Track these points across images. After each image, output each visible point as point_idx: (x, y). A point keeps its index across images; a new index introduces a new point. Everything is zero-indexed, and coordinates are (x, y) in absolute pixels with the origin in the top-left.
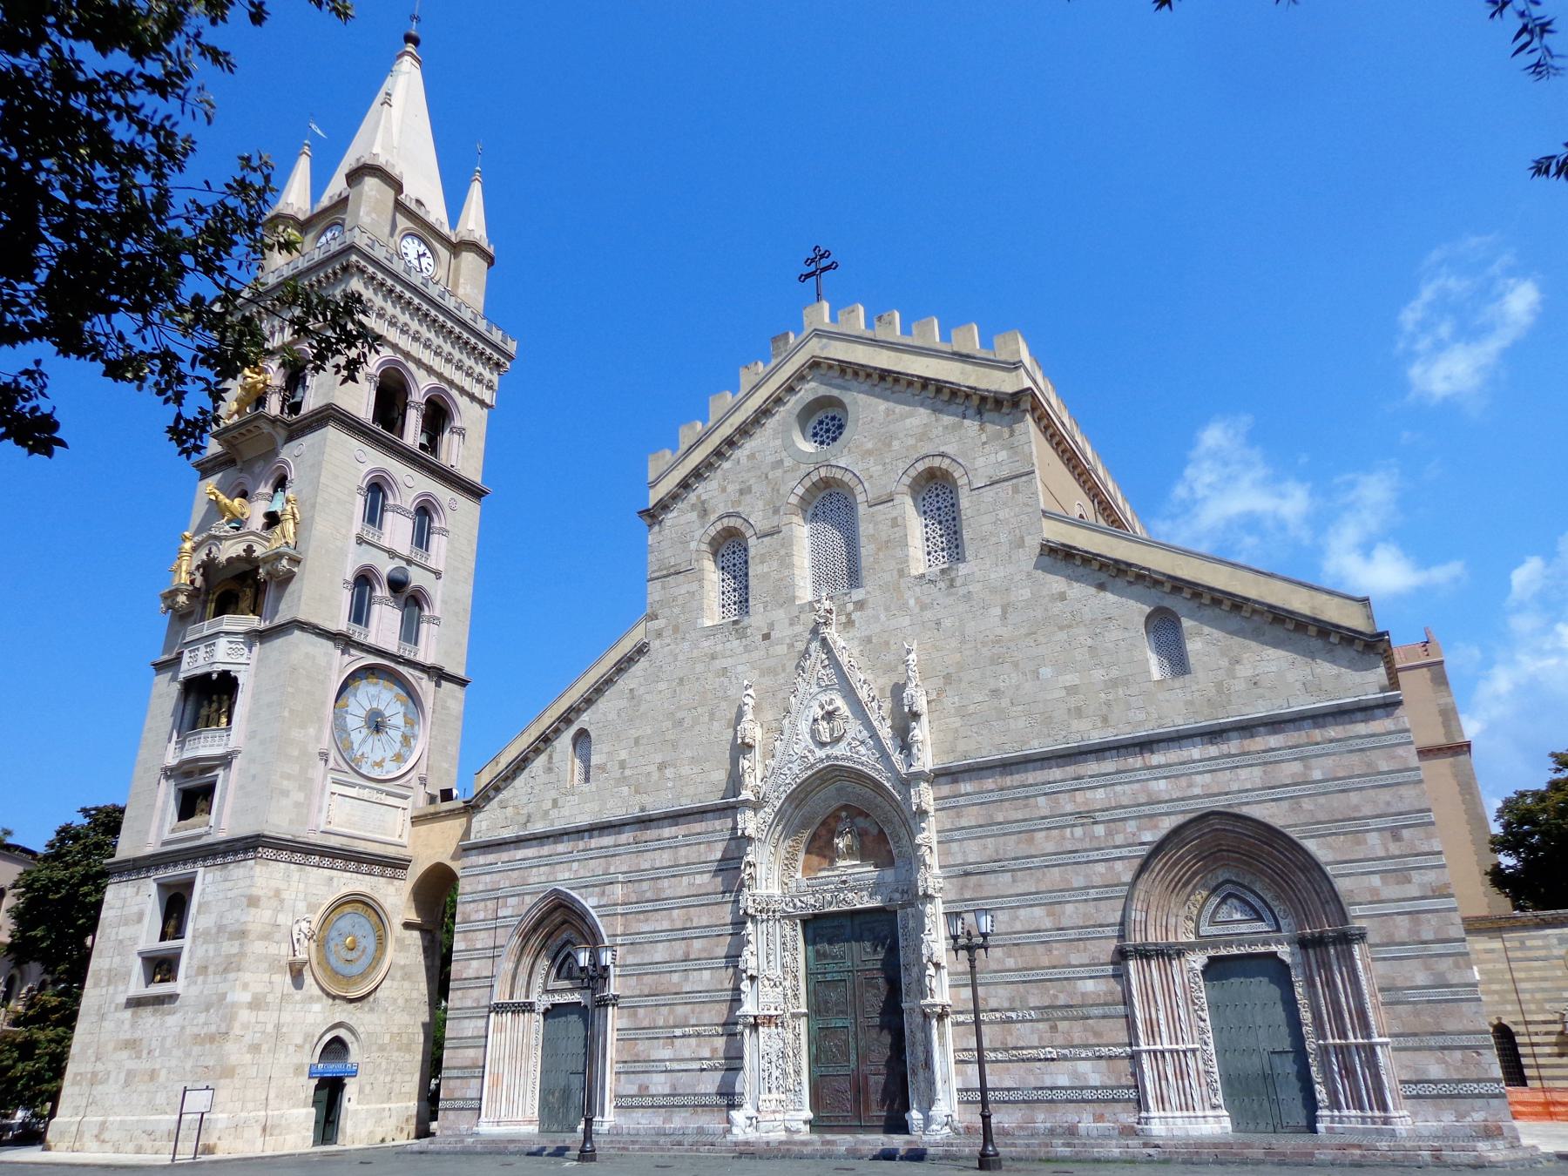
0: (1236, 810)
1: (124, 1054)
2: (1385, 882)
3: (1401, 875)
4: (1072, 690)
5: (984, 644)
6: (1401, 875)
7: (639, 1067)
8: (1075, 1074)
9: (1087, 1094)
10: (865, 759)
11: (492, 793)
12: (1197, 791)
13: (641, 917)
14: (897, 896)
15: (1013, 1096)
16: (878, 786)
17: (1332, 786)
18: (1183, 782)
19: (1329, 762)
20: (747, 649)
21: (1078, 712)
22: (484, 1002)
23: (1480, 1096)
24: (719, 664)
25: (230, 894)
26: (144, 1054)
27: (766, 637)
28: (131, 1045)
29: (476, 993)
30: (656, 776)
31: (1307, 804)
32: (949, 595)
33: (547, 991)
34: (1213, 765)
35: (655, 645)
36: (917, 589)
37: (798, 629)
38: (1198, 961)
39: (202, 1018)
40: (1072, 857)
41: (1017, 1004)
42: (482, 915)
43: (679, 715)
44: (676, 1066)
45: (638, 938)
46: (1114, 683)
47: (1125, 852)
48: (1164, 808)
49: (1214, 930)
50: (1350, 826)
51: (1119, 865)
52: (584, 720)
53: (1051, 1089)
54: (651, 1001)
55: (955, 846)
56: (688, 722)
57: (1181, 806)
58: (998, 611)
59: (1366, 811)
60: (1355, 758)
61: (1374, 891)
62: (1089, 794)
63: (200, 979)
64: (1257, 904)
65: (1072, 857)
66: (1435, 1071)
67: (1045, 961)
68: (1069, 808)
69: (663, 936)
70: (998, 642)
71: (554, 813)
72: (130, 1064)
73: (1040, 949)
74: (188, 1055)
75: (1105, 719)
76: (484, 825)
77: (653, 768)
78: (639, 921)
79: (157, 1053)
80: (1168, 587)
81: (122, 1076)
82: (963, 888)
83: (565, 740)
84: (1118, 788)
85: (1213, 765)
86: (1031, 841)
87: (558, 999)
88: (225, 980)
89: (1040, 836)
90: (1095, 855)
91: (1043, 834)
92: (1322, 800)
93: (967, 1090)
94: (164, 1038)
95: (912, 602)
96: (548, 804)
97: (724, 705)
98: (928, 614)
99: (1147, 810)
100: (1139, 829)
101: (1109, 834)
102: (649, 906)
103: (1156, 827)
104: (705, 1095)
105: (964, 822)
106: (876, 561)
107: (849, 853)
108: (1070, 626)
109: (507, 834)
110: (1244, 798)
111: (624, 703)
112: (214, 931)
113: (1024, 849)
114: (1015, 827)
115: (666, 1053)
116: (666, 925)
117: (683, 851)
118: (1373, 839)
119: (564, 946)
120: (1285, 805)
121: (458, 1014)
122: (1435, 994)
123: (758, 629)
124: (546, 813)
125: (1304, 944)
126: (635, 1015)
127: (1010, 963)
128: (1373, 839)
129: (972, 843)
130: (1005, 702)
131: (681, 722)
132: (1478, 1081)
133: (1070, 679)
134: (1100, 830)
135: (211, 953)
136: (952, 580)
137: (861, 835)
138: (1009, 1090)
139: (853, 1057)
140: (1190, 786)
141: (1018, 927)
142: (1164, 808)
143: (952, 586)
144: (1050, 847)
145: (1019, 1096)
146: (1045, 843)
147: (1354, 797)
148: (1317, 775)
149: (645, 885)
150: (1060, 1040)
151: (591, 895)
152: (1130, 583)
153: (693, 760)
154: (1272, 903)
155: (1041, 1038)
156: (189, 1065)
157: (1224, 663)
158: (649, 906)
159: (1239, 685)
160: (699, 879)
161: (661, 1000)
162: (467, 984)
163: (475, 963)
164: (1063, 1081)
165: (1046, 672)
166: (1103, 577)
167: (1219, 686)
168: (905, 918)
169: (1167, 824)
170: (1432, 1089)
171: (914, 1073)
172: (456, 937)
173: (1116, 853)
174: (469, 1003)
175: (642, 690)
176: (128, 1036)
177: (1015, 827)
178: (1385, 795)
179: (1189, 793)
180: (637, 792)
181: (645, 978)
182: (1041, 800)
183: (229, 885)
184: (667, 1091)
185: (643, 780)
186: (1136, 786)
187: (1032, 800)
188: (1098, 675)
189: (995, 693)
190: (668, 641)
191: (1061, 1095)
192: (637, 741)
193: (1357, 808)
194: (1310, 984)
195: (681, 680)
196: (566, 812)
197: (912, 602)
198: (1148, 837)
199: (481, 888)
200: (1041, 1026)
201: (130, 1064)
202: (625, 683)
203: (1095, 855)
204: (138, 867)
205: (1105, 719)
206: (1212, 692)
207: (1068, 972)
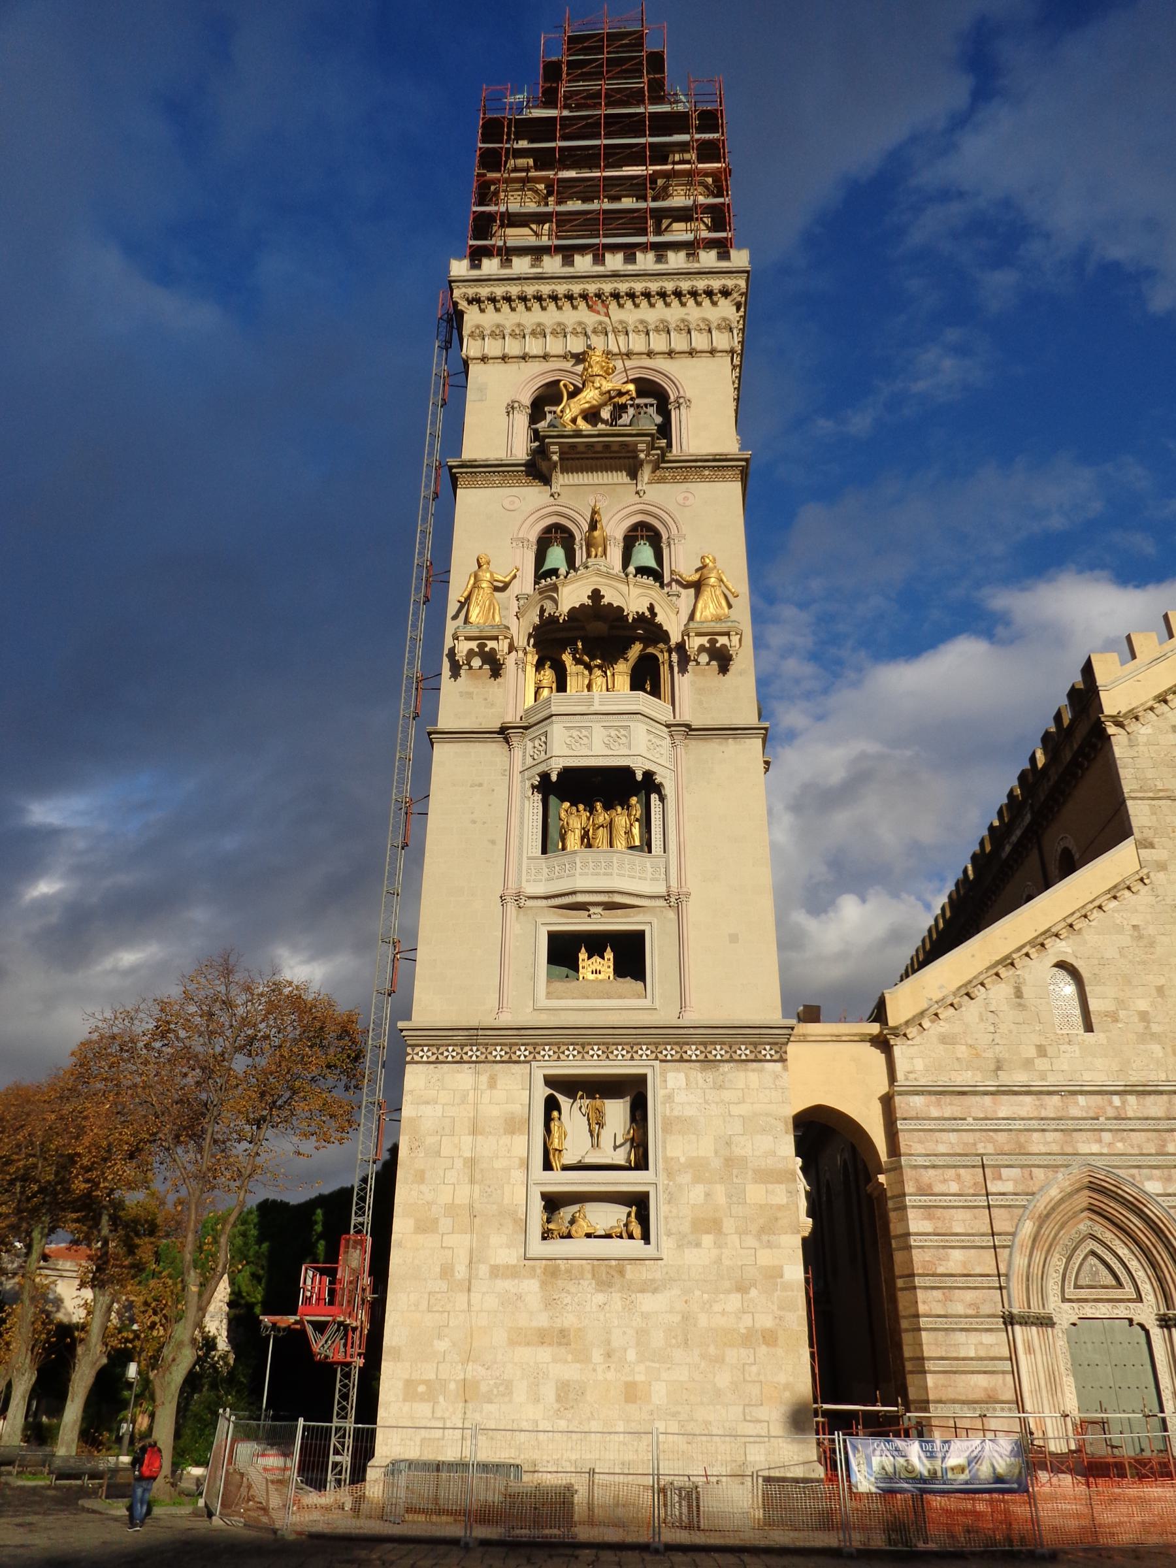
1: (544, 1354)
11: (926, 1023)
22: (986, 1309)
25: (735, 1110)
26: (597, 1356)
28: (562, 1337)
29: (969, 1296)
33: (1065, 1300)
35: (1158, 877)
39: (734, 1301)
42: (954, 1188)
63: (707, 1240)
71: (1041, 1064)
72: (571, 1372)
74: (720, 1360)
76: (919, 1065)
79: (631, 1355)
81: (549, 1393)
87: (1089, 1310)
88: (769, 1245)
96: (1032, 1052)
109: (965, 1078)
111: (1125, 940)
112: (716, 1163)
119: (1082, 1240)
121: (941, 1323)
124: (1028, 1064)
135: (721, 1199)
151: (1149, 1178)
156: (723, 1379)
162: (949, 1282)
163: (957, 1254)
172: (911, 1214)
174: (960, 1309)
175: (1151, 930)
176: (543, 1320)
183: (727, 1095)
192: (1160, 990)
196: (1063, 1064)
199: (942, 1149)
201: (571, 1372)
204: (474, 1043)
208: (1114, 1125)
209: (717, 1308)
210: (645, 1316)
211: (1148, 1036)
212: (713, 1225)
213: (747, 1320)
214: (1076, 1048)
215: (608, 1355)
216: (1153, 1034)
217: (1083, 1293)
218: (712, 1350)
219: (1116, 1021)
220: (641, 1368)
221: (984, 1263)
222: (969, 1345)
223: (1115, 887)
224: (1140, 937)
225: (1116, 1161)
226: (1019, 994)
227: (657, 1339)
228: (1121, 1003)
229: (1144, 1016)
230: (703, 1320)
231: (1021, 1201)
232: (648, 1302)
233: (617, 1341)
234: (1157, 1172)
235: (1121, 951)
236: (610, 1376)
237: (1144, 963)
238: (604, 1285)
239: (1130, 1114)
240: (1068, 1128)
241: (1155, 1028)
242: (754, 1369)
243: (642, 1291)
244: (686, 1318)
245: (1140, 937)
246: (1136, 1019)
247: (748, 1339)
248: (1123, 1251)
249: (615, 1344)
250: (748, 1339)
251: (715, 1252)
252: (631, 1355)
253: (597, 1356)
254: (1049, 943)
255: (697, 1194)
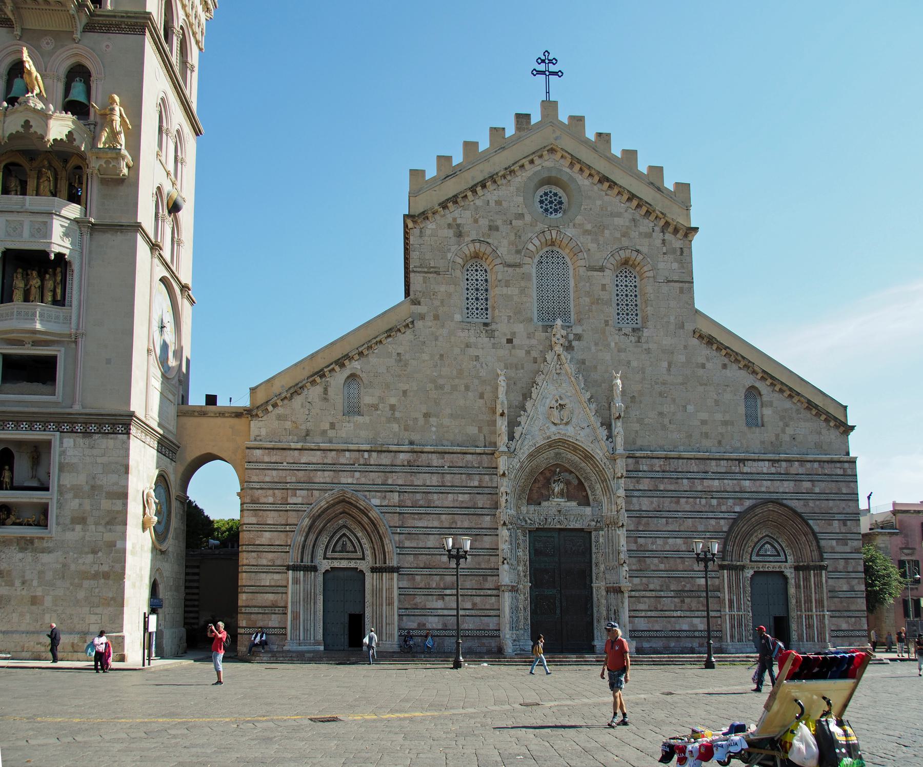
0: (785, 502)
2: (837, 544)
3: (844, 541)
4: (704, 422)
5: (657, 383)
6: (844, 541)
7: (417, 612)
8: (692, 625)
9: (697, 634)
10: (582, 438)
12: (763, 489)
13: (416, 516)
14: (594, 523)
15: (659, 634)
16: (588, 457)
17: (823, 497)
18: (758, 482)
19: (823, 485)
20: (494, 346)
21: (706, 435)
23: (859, 636)
24: (472, 352)
26: (18, 583)
27: (510, 341)
30: (421, 421)
31: (811, 504)
32: (637, 346)
34: (772, 477)
36: (617, 337)
37: (534, 342)
38: (749, 573)
40: (696, 515)
41: (664, 588)
43: (441, 382)
44: (446, 612)
45: (413, 531)
46: (725, 423)
47: (726, 515)
48: (747, 495)
49: (758, 559)
50: (827, 517)
51: (722, 522)
52: (355, 366)
53: (679, 631)
54: (425, 571)
55: (635, 500)
56: (447, 388)
57: (755, 495)
58: (665, 364)
59: (835, 511)
60: (834, 484)
61: (832, 547)
62: (710, 482)
64: (779, 548)
65: (696, 515)
66: (844, 626)
67: (681, 567)
68: (699, 488)
69: (435, 531)
70: (664, 384)
73: (679, 561)
74: (80, 586)
75: (720, 442)
77: (420, 416)
78: (414, 519)
79: (35, 583)
80: (759, 376)
82: (639, 523)
83: (340, 376)
84: (726, 481)
85: (772, 477)
86: (678, 503)
89: (683, 501)
90: (711, 515)
91: (685, 500)
92: (818, 503)
93: (634, 631)
94: (41, 573)
95: (613, 344)
97: (476, 382)
98: (623, 355)
99: (739, 495)
100: (734, 504)
101: (719, 505)
102: (422, 510)
103: (742, 505)
104: (468, 630)
105: (641, 487)
106: (590, 310)
107: (561, 494)
108: (706, 385)
110: (785, 496)
113: (674, 507)
114: (669, 494)
115: (440, 604)
116: (436, 524)
117: (448, 477)
118: (836, 523)
120: (802, 502)
122: (848, 595)
123: (505, 334)
125: (797, 568)
126: (414, 580)
127: (662, 567)
128: (836, 523)
129: (645, 499)
130: (666, 421)
131: (441, 387)
132: (858, 631)
133: (704, 416)
134: (714, 502)
136: (639, 338)
137: (568, 483)
138: (657, 631)
139: (558, 611)
140: (760, 486)
141: (667, 548)
142: (747, 495)
143: (639, 342)
144: (688, 508)
145: (663, 634)
146: (684, 505)
147: (831, 503)
148: (817, 490)
149: (418, 496)
150: (685, 607)
152: (740, 368)
153: (451, 416)
154: (786, 549)
155: (675, 606)
156: (81, 594)
157: (781, 424)
158: (422, 510)
159: (786, 438)
160: (461, 498)
161: (434, 571)
164: (685, 627)
165: (690, 408)
166: (726, 361)
167: (777, 436)
168: (597, 537)
169: (748, 503)
170: (841, 634)
171: (598, 621)
173: (722, 515)
175: (407, 357)
177: (669, 494)
178: (843, 504)
179: (759, 490)
180: (406, 430)
181: (420, 557)
182: (685, 481)
184: (440, 627)
185: (410, 423)
186: (735, 482)
187: (680, 481)
188: (719, 417)
189: (661, 414)
190: (430, 324)
191: (684, 634)
192: (405, 392)
193: (831, 508)
194: (798, 586)
195: (442, 356)
197: (613, 344)
198: (737, 509)
200: (676, 600)
202: (391, 346)
203: (711, 515)
205: (720, 442)
206: (773, 439)
207: (692, 574)
208: (362, 468)
209: (80, 561)
210: (42, 564)
211: (393, 419)
212: (80, 520)
213: (96, 567)
214: (352, 425)
215: (23, 583)
216: (395, 418)
217: (336, 555)
218: (76, 581)
219: (377, 409)
220: (40, 589)
221: (279, 539)
222: (266, 580)
223: (390, 329)
224: (400, 360)
225: (358, 487)
226: (326, 390)
227: (49, 575)
228: (382, 399)
229: (393, 408)
230: (73, 567)
231: (304, 507)
232: (45, 558)
233: (28, 576)
234: (378, 494)
235: (388, 368)
236: (24, 593)
237: (400, 376)
238: (22, 549)
239: (372, 462)
240: (336, 468)
241: (397, 414)
242: (97, 590)
243: (43, 552)
244: (64, 565)
245: (400, 360)
246: (388, 409)
247: (95, 576)
248: (360, 534)
249: (27, 578)
250: (95, 576)
251: (82, 534)
252: (35, 583)
253: (18, 583)
254: (347, 362)
255: (75, 504)
